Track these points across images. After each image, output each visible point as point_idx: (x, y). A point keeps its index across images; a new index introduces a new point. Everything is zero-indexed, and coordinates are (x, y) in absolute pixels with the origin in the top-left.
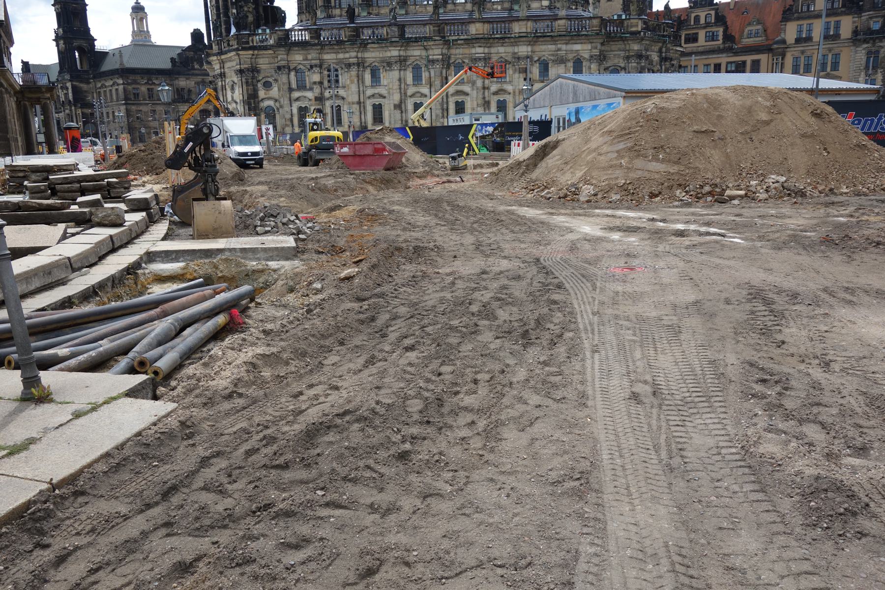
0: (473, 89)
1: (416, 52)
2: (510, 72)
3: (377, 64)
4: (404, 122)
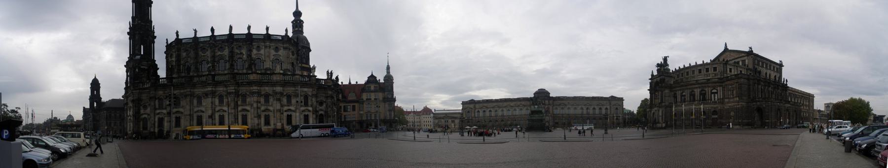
0: (251, 109)
1: (221, 89)
2: (271, 100)
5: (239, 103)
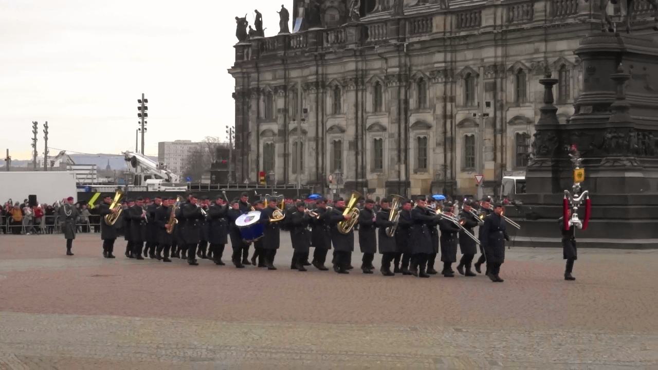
4: (359, 170)
5: (413, 103)
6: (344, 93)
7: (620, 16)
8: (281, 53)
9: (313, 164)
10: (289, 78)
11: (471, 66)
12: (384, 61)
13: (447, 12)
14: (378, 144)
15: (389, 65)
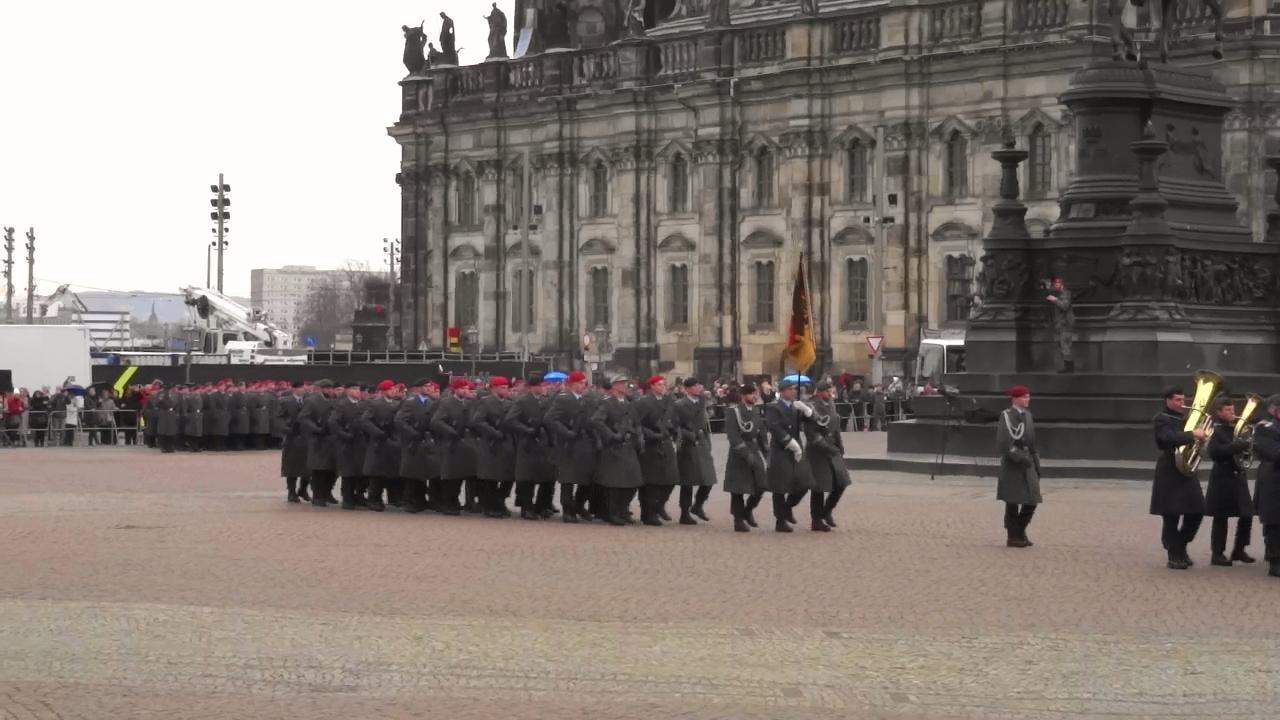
3: (601, 157)
5: (746, 196)
6: (612, 176)
7: (1148, 30)
8: (490, 97)
9: (553, 315)
10: (506, 146)
11: (861, 126)
12: (692, 114)
13: (813, 20)
14: (679, 274)
15: (702, 121)
